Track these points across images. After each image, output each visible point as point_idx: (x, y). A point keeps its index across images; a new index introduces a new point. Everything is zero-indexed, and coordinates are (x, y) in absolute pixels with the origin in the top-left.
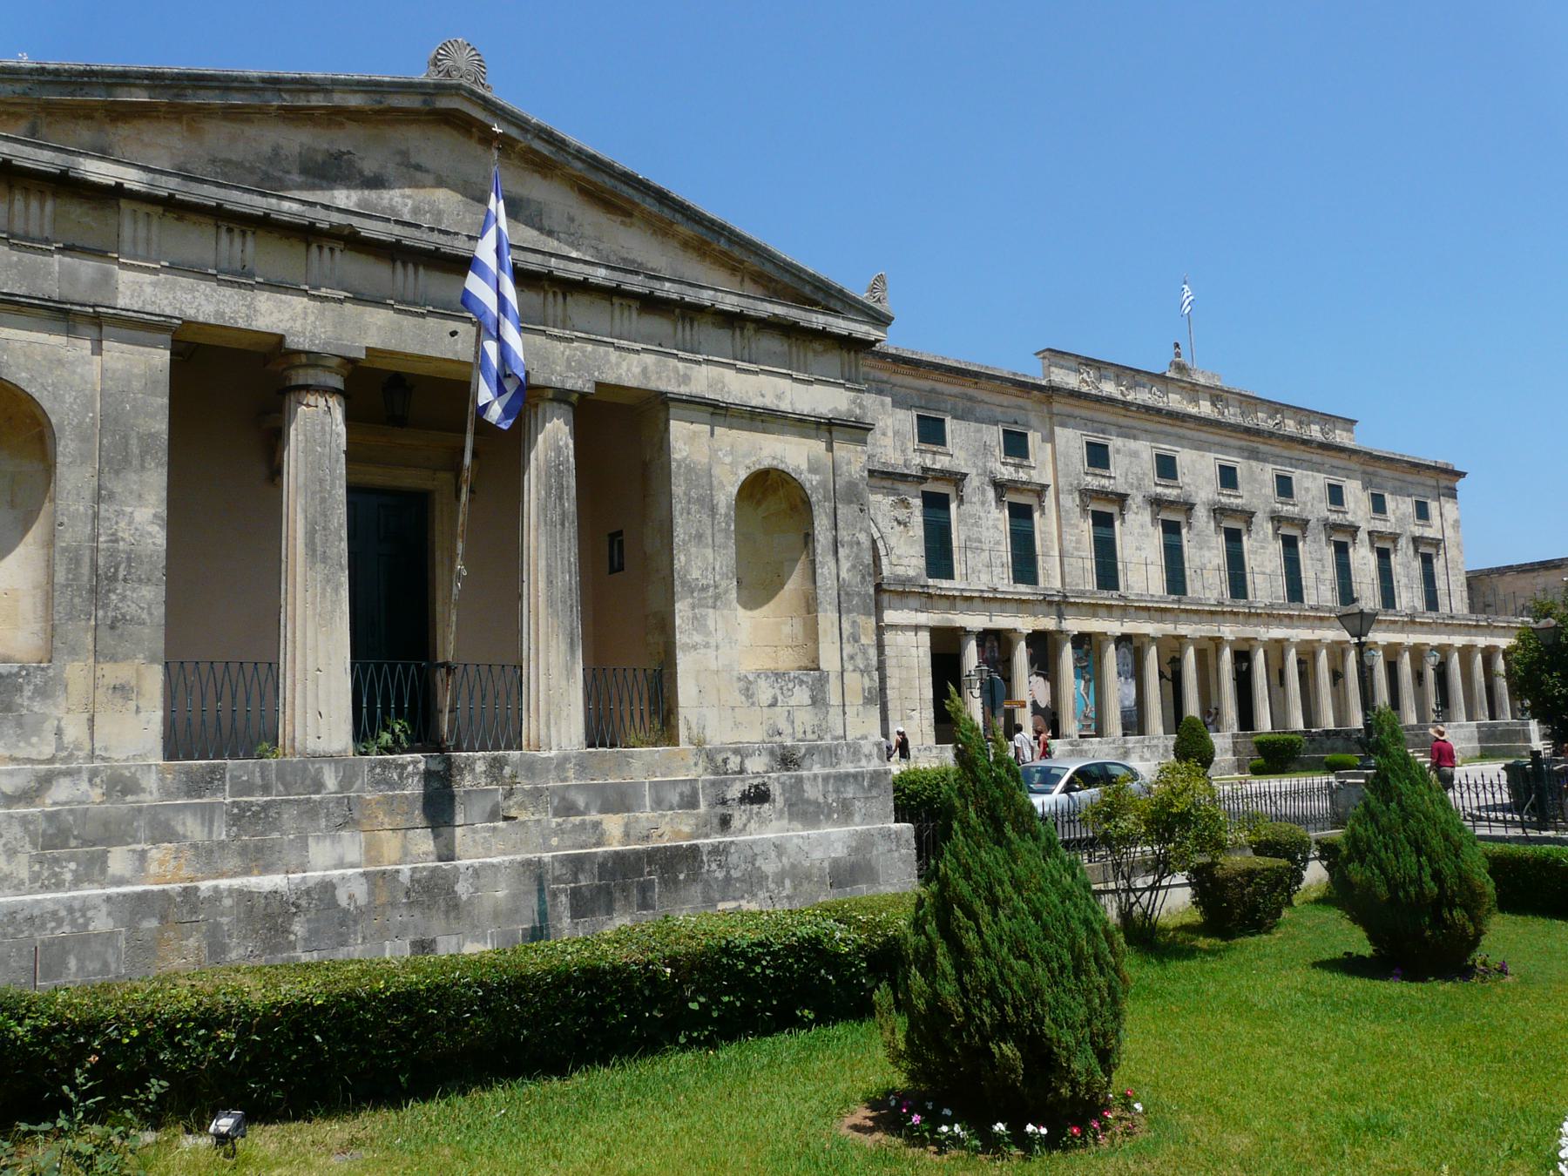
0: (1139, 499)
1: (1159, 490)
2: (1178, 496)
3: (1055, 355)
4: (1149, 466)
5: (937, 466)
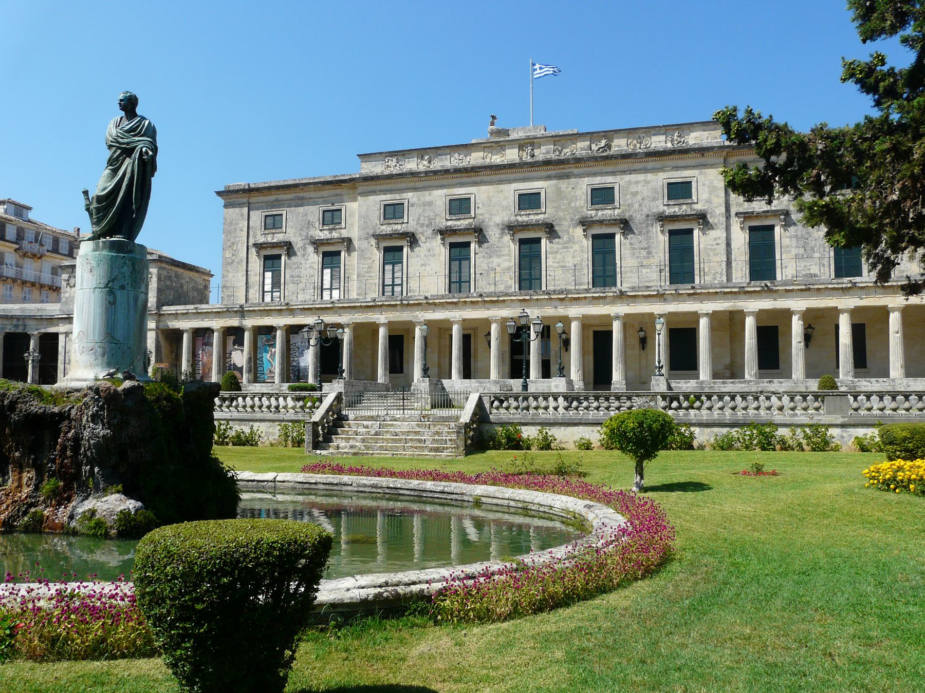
0: (429, 232)
1: (449, 223)
2: (470, 224)
3: (365, 157)
4: (443, 208)
5: (275, 241)
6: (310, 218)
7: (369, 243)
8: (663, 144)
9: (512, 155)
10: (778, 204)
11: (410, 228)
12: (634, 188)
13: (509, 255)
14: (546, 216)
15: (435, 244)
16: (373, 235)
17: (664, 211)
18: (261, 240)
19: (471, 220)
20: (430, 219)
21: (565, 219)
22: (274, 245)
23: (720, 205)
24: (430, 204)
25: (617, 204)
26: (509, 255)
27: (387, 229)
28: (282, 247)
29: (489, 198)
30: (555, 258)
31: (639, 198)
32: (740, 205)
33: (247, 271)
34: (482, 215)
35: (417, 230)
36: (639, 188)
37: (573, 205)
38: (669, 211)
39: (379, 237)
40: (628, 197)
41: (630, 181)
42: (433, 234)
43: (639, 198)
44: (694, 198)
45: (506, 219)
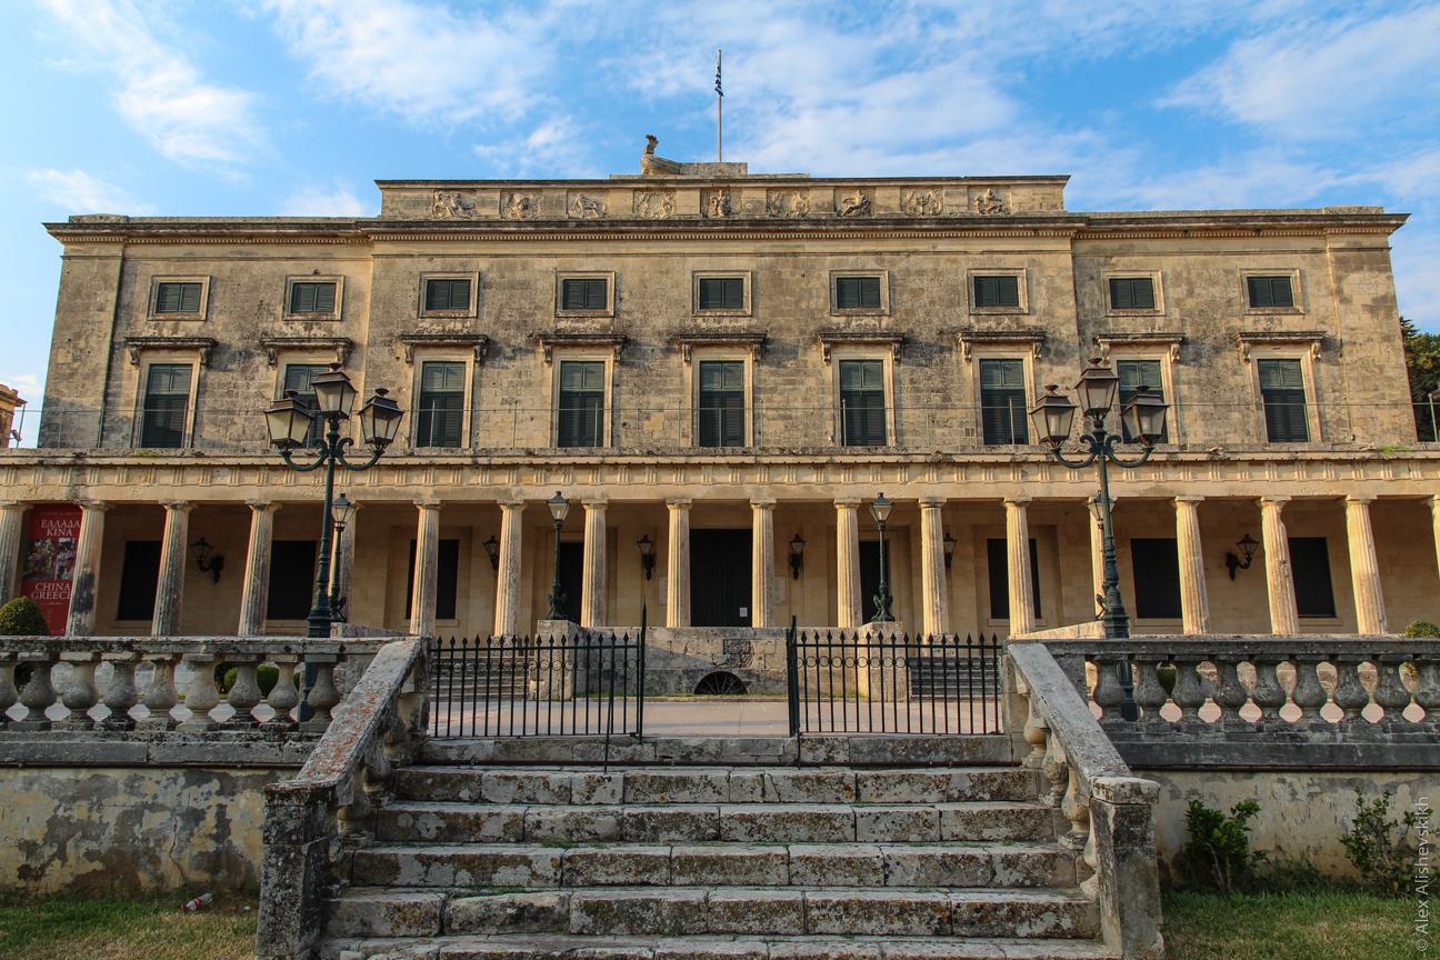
0: (521, 340)
1: (563, 324)
2: (605, 328)
5: (181, 335)
6: (266, 297)
7: (392, 352)
8: (963, 209)
9: (686, 203)
10: (1165, 326)
11: (486, 326)
12: (914, 283)
13: (681, 391)
14: (754, 321)
15: (532, 363)
16: (403, 337)
17: (970, 326)
18: (149, 332)
19: (607, 321)
20: (522, 314)
21: (789, 330)
22: (175, 346)
23: (1068, 321)
24: (525, 285)
25: (885, 308)
26: (681, 391)
27: (430, 326)
28: (196, 349)
29: (643, 283)
30: (770, 401)
31: (925, 299)
32: (1098, 323)
33: (106, 395)
34: (629, 313)
35: (495, 333)
36: (925, 283)
37: (803, 305)
39: (419, 342)
40: (905, 297)
41: (908, 272)
42: (528, 342)
43: (925, 299)
44: (1023, 304)
45: (676, 323)
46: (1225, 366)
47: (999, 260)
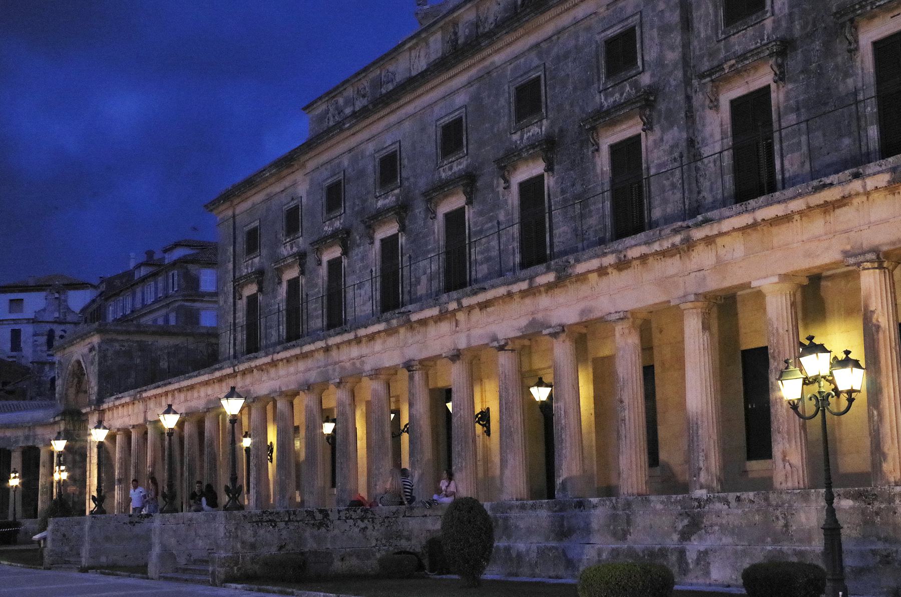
1: (380, 203)
19: (397, 191)
34: (408, 179)
37: (495, 130)
38: (607, 103)
41: (558, 59)
46: (836, 67)
47: (622, 9)
